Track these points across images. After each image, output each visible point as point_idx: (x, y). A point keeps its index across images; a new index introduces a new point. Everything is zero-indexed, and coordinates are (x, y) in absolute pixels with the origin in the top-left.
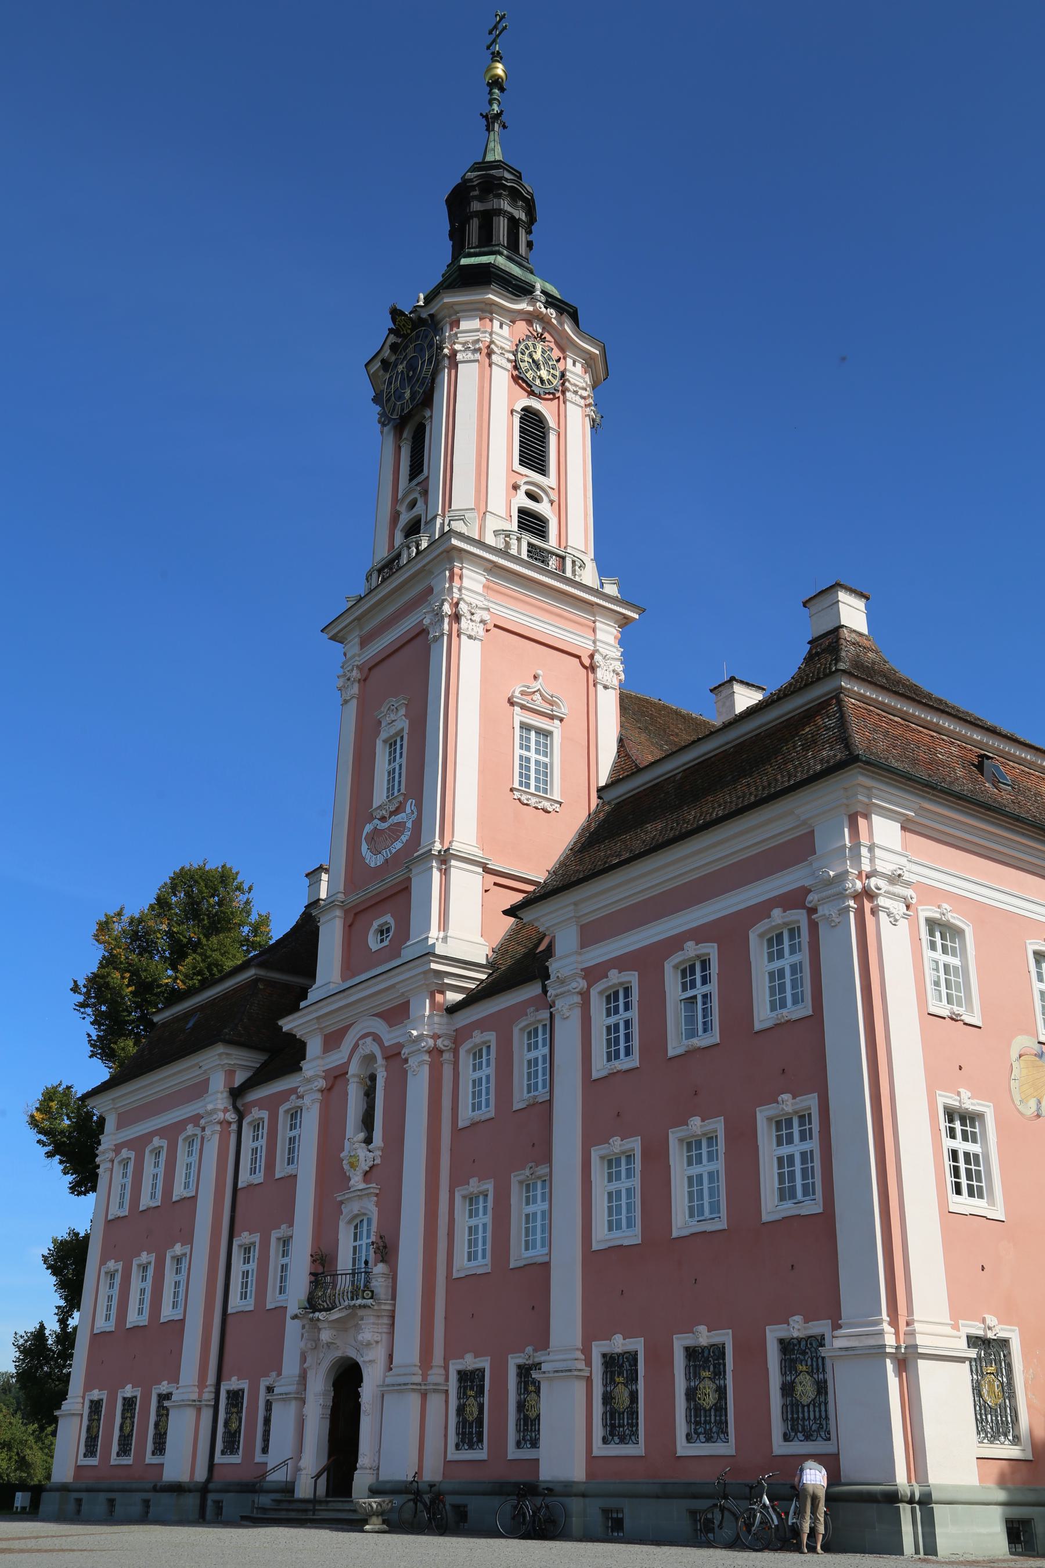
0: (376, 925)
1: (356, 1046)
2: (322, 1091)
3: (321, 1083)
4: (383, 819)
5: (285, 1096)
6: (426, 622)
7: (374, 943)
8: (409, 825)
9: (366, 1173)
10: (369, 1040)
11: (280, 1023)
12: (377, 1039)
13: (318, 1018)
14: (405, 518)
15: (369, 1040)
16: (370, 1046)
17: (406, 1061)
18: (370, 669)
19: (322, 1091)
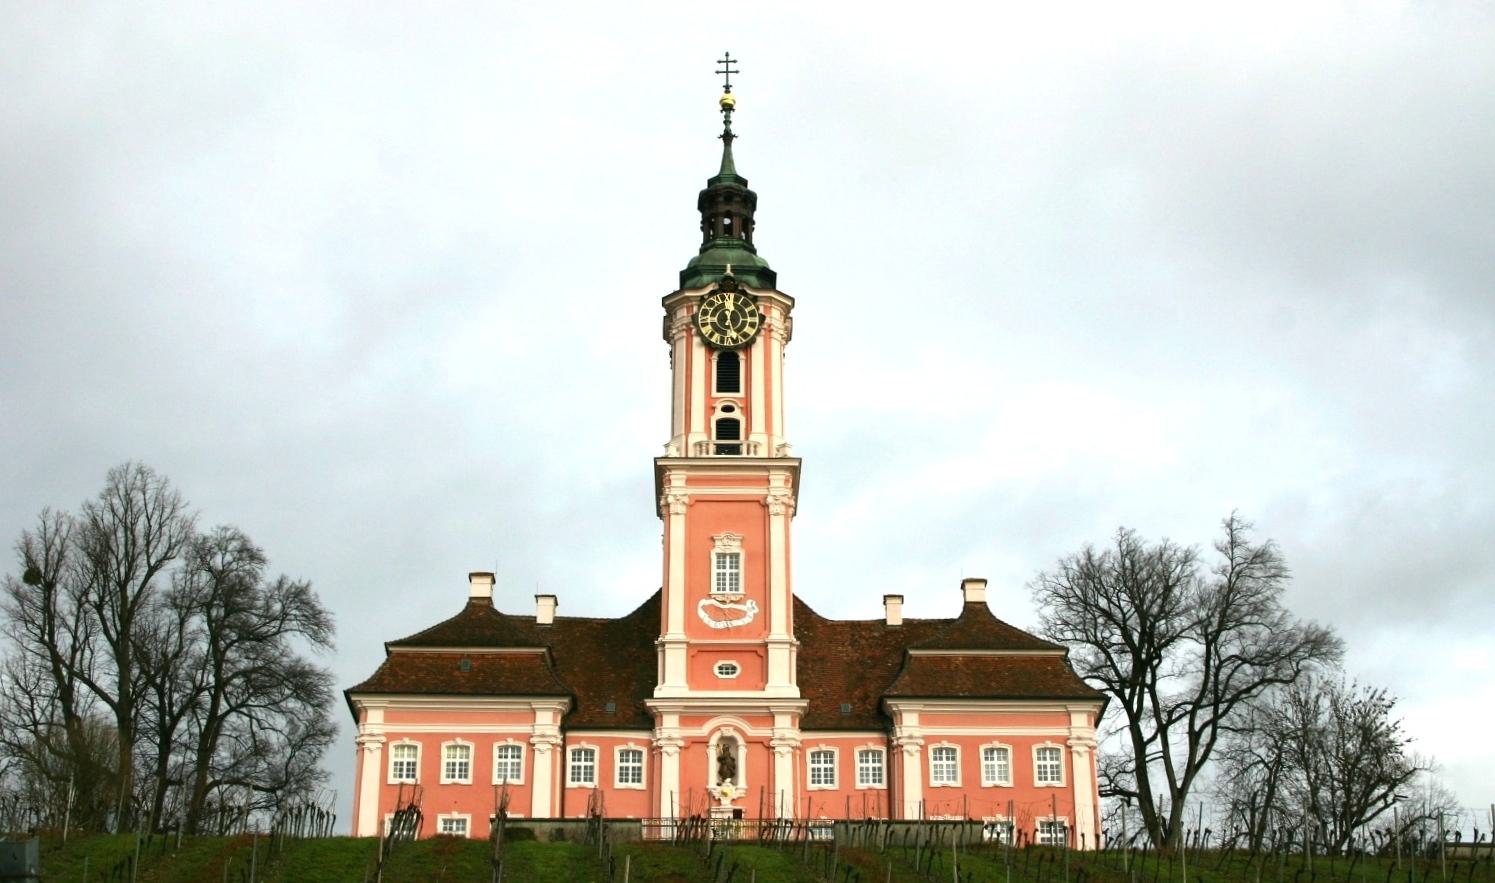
0: (720, 663)
1: (718, 729)
2: (680, 748)
3: (681, 743)
4: (723, 602)
5: (625, 741)
6: (770, 500)
7: (716, 671)
8: (751, 614)
9: (733, 800)
10: (731, 729)
11: (646, 700)
12: (737, 729)
13: (686, 707)
14: (720, 415)
15: (731, 729)
16: (729, 732)
17: (774, 748)
18: (697, 501)
19: (680, 748)
